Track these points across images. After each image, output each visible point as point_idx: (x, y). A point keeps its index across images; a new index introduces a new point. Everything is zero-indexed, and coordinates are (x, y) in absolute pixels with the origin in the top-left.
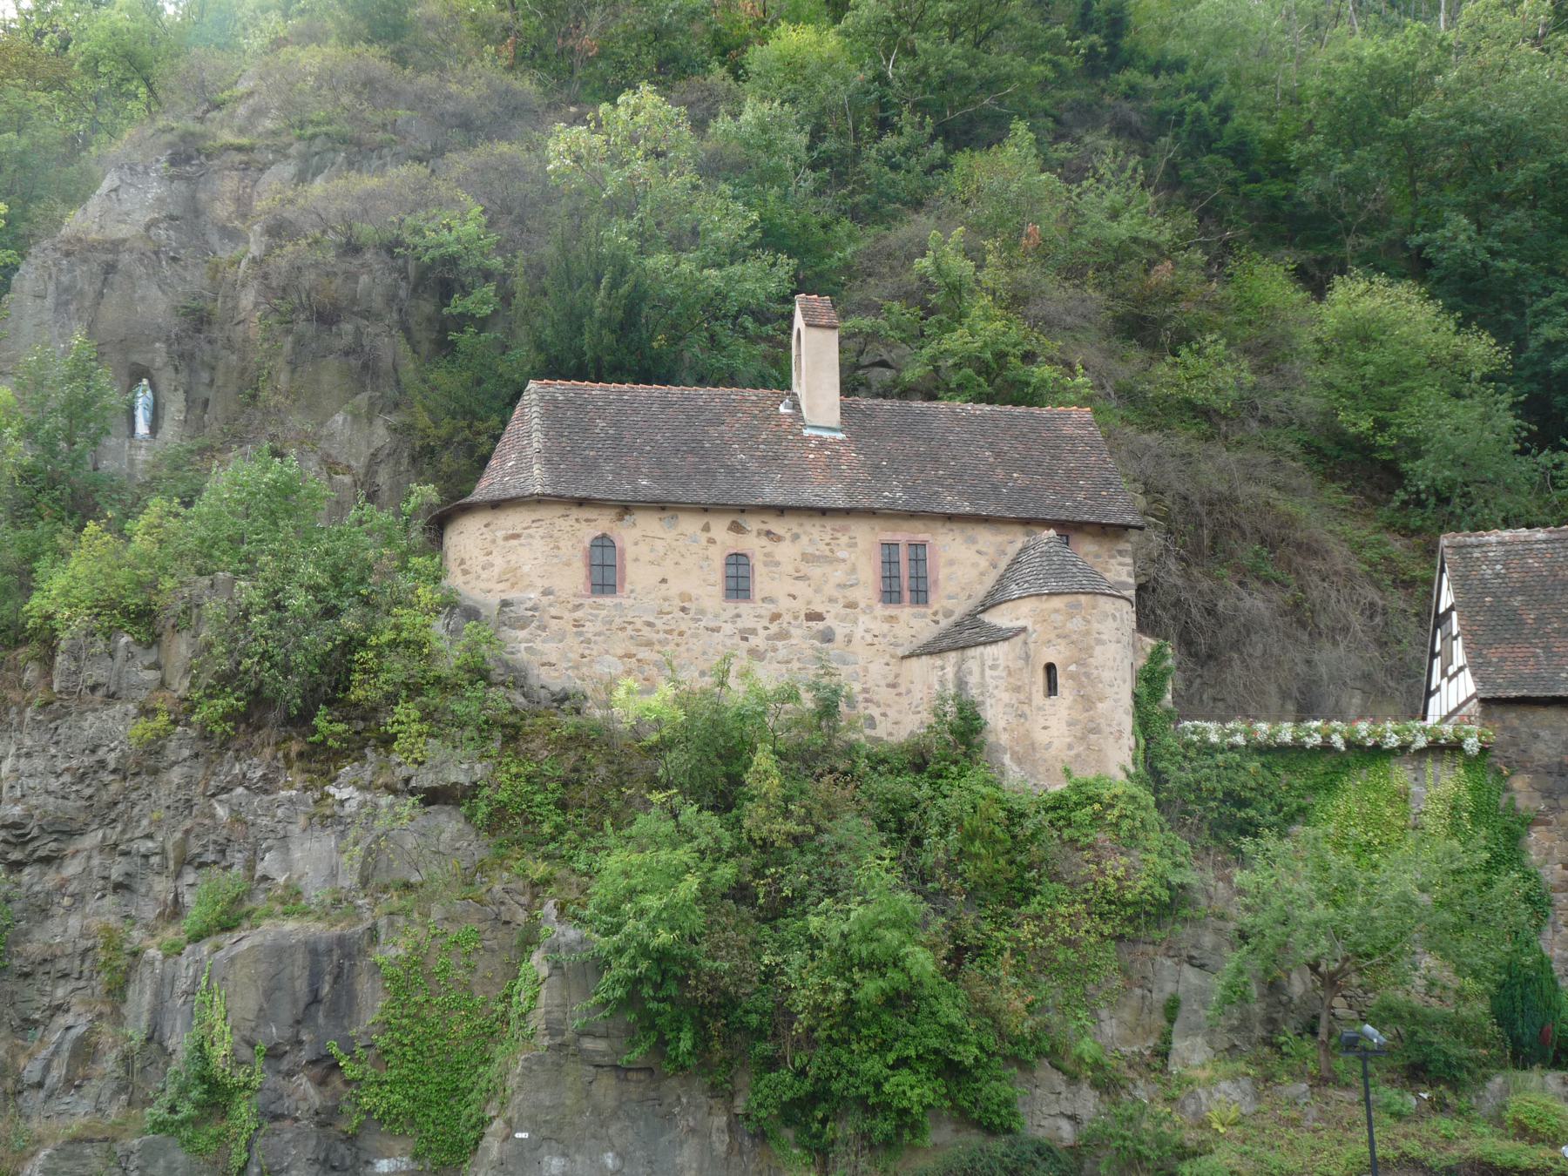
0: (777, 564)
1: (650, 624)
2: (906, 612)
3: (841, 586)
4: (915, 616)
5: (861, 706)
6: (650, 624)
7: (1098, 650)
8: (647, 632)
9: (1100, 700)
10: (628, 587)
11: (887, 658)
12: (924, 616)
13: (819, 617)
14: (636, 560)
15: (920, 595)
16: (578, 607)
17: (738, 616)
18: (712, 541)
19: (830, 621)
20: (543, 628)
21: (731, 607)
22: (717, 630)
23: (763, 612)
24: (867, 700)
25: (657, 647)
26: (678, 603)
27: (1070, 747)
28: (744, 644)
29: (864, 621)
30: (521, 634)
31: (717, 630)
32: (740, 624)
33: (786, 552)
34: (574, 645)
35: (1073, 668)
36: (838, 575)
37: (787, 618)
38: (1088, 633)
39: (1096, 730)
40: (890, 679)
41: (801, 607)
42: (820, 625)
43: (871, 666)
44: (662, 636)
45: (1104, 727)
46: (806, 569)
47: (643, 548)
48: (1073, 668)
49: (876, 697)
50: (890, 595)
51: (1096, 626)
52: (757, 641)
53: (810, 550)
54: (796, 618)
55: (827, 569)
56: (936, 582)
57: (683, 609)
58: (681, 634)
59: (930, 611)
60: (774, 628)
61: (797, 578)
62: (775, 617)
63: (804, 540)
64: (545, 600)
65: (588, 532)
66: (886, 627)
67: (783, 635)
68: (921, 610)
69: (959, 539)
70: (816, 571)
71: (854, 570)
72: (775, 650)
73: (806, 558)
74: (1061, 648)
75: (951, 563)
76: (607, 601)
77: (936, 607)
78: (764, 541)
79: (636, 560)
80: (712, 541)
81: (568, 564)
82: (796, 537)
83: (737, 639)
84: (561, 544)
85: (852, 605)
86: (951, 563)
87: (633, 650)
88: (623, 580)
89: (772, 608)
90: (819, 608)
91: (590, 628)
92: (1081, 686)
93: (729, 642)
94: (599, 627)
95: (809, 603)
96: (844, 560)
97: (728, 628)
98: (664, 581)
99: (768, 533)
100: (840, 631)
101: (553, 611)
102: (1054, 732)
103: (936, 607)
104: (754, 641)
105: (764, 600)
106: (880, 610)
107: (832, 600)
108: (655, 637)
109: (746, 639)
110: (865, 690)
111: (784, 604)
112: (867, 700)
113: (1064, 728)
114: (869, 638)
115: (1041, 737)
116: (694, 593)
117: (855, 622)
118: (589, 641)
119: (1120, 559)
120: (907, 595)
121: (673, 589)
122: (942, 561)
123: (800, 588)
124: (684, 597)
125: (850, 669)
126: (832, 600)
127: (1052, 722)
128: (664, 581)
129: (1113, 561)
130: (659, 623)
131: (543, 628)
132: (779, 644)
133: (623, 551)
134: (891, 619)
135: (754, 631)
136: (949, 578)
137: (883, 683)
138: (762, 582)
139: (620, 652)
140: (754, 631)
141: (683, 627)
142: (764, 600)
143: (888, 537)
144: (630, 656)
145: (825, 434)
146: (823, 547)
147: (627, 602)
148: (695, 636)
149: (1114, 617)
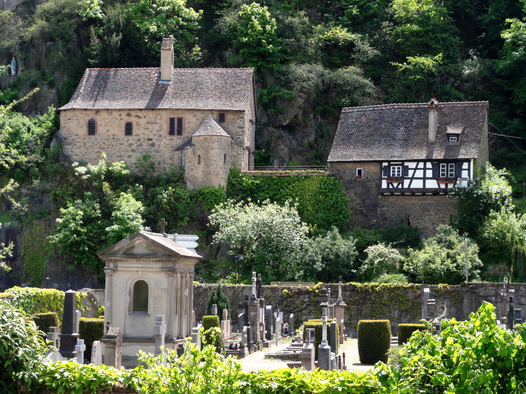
0: (140, 125)
1: (104, 143)
2: (175, 138)
3: (157, 131)
4: (178, 138)
5: (162, 165)
6: (104, 143)
7: (212, 151)
8: (103, 146)
9: (212, 165)
10: (98, 133)
11: (170, 151)
12: (181, 138)
13: (151, 140)
14: (101, 125)
15: (180, 133)
16: (84, 139)
17: (128, 140)
18: (122, 119)
19: (154, 141)
20: (75, 145)
21: (127, 138)
22: (123, 144)
23: (135, 139)
24: (164, 163)
25: (106, 149)
26: (112, 137)
27: (203, 178)
28: (130, 148)
29: (164, 140)
30: (70, 147)
31: (123, 144)
32: (129, 142)
33: (142, 121)
34: (83, 149)
35: (204, 156)
36: (157, 127)
37: (142, 140)
38: (208, 147)
39: (210, 174)
40: (171, 157)
41: (146, 137)
42: (151, 142)
43: (165, 153)
44: (107, 146)
45: (212, 172)
46: (148, 126)
47: (103, 121)
48: (204, 156)
49: (166, 162)
50: (171, 133)
51: (211, 145)
52: (133, 147)
53: (149, 120)
54: (145, 140)
55: (154, 126)
56: (185, 128)
57: (113, 139)
58: (113, 146)
59: (182, 137)
60: (138, 143)
61: (145, 129)
62: (139, 140)
63: (148, 118)
64: (76, 137)
65: (88, 118)
66: (170, 142)
67: (141, 145)
68: (180, 137)
69: (192, 115)
70: (150, 126)
71: (161, 126)
72: (138, 149)
73: (148, 123)
74: (202, 151)
75: (189, 123)
76: (92, 137)
77: (184, 136)
78: (136, 118)
79: (101, 125)
80: (122, 119)
81: (82, 127)
82: (145, 117)
83: (128, 146)
84: (81, 121)
85: (161, 136)
86: (189, 123)
87: (99, 150)
88: (97, 131)
89: (138, 138)
90: (151, 137)
91: (88, 145)
92: (206, 161)
93: (126, 147)
94: (90, 144)
95: (148, 136)
96: (158, 123)
97: (125, 144)
98: (108, 131)
99: (138, 116)
100: (157, 143)
101: (78, 140)
102: (199, 174)
103: (184, 136)
104: (133, 147)
105: (136, 135)
106: (169, 137)
107: (155, 135)
108: (105, 147)
109: (130, 146)
110: (164, 160)
111: (141, 136)
112: (164, 163)
113: (201, 173)
114: (165, 145)
115: (197, 175)
116: (116, 134)
117: (161, 141)
118: (87, 148)
119: (241, 120)
120: (176, 132)
121: (111, 133)
122: (186, 122)
123: (146, 132)
124: (114, 135)
125: (159, 154)
126: (155, 135)
127: (199, 171)
128: (108, 131)
129: (238, 120)
130: (107, 143)
131: (75, 145)
132: (140, 148)
133: (97, 123)
134: (171, 140)
135: (133, 144)
136: (189, 127)
137: (168, 158)
138: (135, 130)
139: (96, 151)
140: (133, 144)
141: (113, 143)
142: (136, 135)
143: (172, 116)
144: (98, 152)
145: (165, 83)
146: (153, 119)
147: (98, 137)
148: (116, 146)
149: (218, 142)
